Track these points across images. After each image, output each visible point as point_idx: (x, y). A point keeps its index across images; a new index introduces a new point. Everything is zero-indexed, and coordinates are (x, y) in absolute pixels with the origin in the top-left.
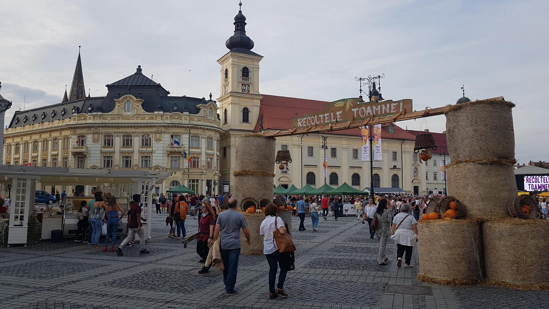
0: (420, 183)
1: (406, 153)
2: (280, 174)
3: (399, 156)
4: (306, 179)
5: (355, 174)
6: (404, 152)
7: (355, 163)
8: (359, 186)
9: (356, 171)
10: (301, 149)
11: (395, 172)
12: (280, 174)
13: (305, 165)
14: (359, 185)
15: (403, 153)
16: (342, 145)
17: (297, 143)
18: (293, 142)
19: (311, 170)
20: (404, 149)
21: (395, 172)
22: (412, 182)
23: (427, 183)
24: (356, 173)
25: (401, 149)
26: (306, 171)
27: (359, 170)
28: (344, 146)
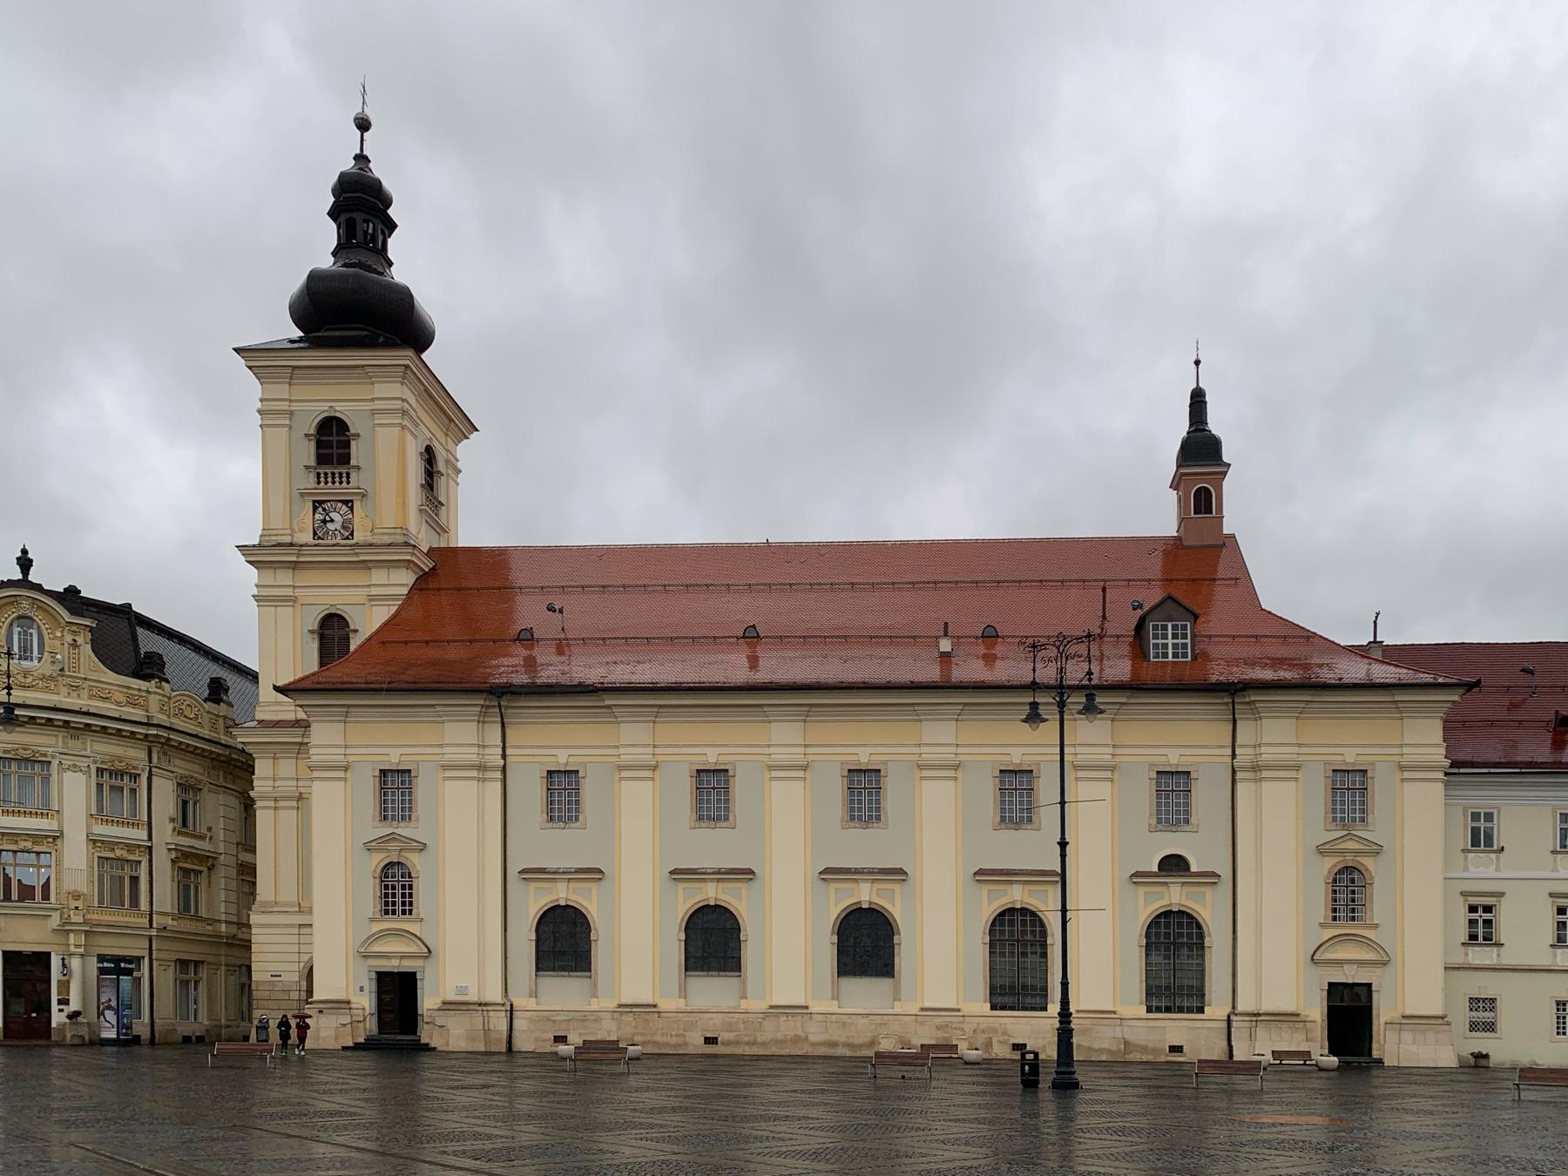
0: (1385, 964)
1: (1265, 774)
2: (372, 920)
3: (1207, 798)
4: (534, 943)
5: (861, 908)
6: (1244, 769)
7: (863, 848)
8: (890, 980)
9: (865, 894)
10: (498, 786)
11: (1175, 895)
12: (372, 920)
13: (522, 872)
14: (892, 976)
15: (1239, 775)
16: (766, 750)
17: (471, 755)
18: (446, 750)
19: (562, 894)
20: (1250, 751)
21: (1175, 895)
22: (1312, 959)
23: (1445, 968)
24: (865, 906)
25: (1229, 752)
26: (532, 903)
27: (893, 890)
28: (780, 755)
